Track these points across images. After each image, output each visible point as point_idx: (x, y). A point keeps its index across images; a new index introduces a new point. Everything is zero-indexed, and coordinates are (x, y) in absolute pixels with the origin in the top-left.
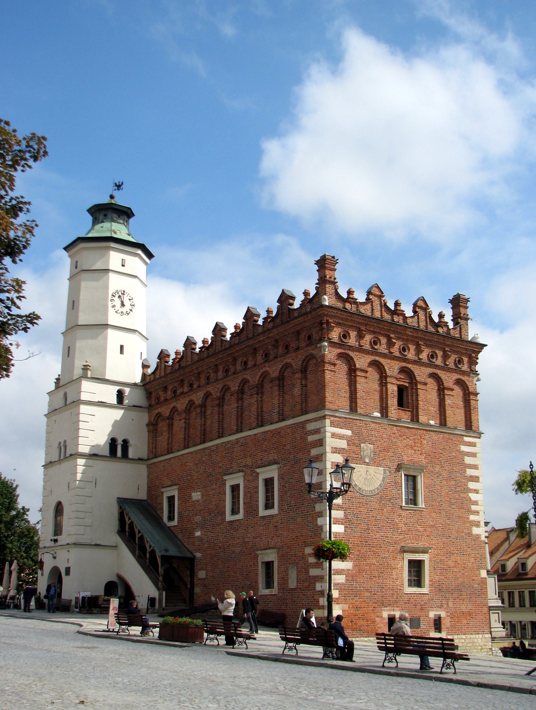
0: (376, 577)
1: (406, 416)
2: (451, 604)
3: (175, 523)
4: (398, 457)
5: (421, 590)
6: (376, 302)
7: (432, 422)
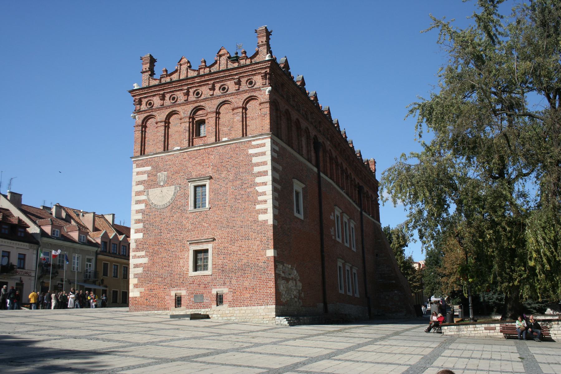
0: (166, 266)
2: (234, 282)
4: (187, 175)
5: (203, 273)
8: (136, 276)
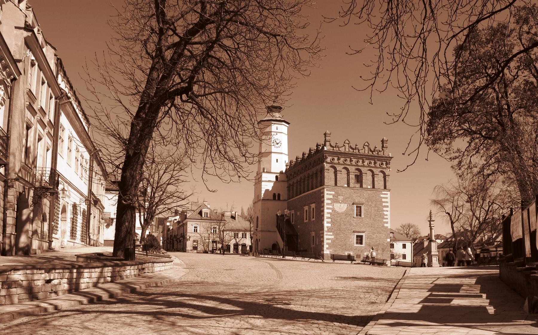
1: (358, 185)
3: (293, 223)
6: (347, 146)
7: (369, 187)
8: (327, 244)
